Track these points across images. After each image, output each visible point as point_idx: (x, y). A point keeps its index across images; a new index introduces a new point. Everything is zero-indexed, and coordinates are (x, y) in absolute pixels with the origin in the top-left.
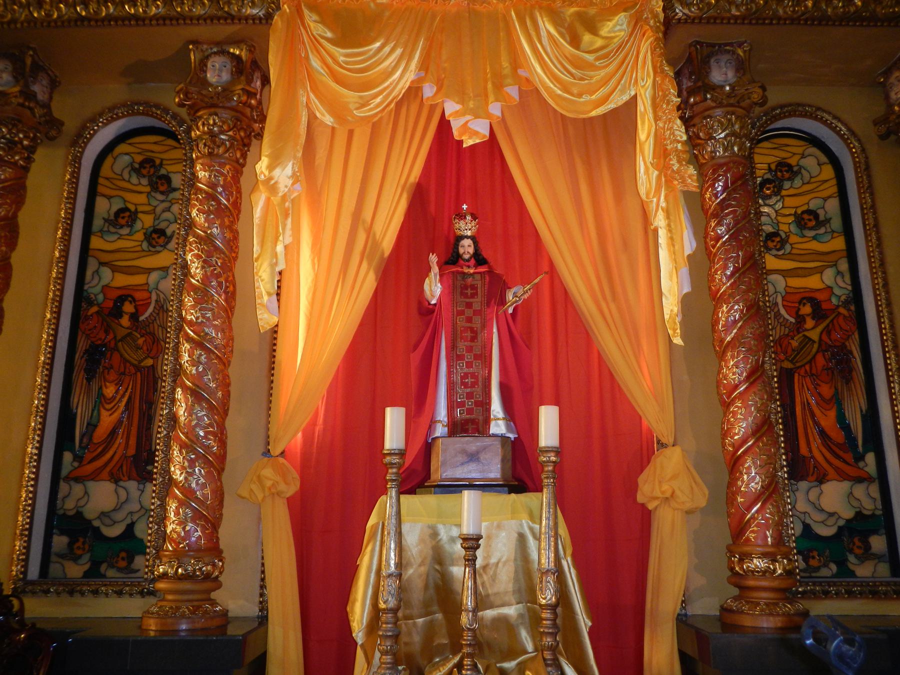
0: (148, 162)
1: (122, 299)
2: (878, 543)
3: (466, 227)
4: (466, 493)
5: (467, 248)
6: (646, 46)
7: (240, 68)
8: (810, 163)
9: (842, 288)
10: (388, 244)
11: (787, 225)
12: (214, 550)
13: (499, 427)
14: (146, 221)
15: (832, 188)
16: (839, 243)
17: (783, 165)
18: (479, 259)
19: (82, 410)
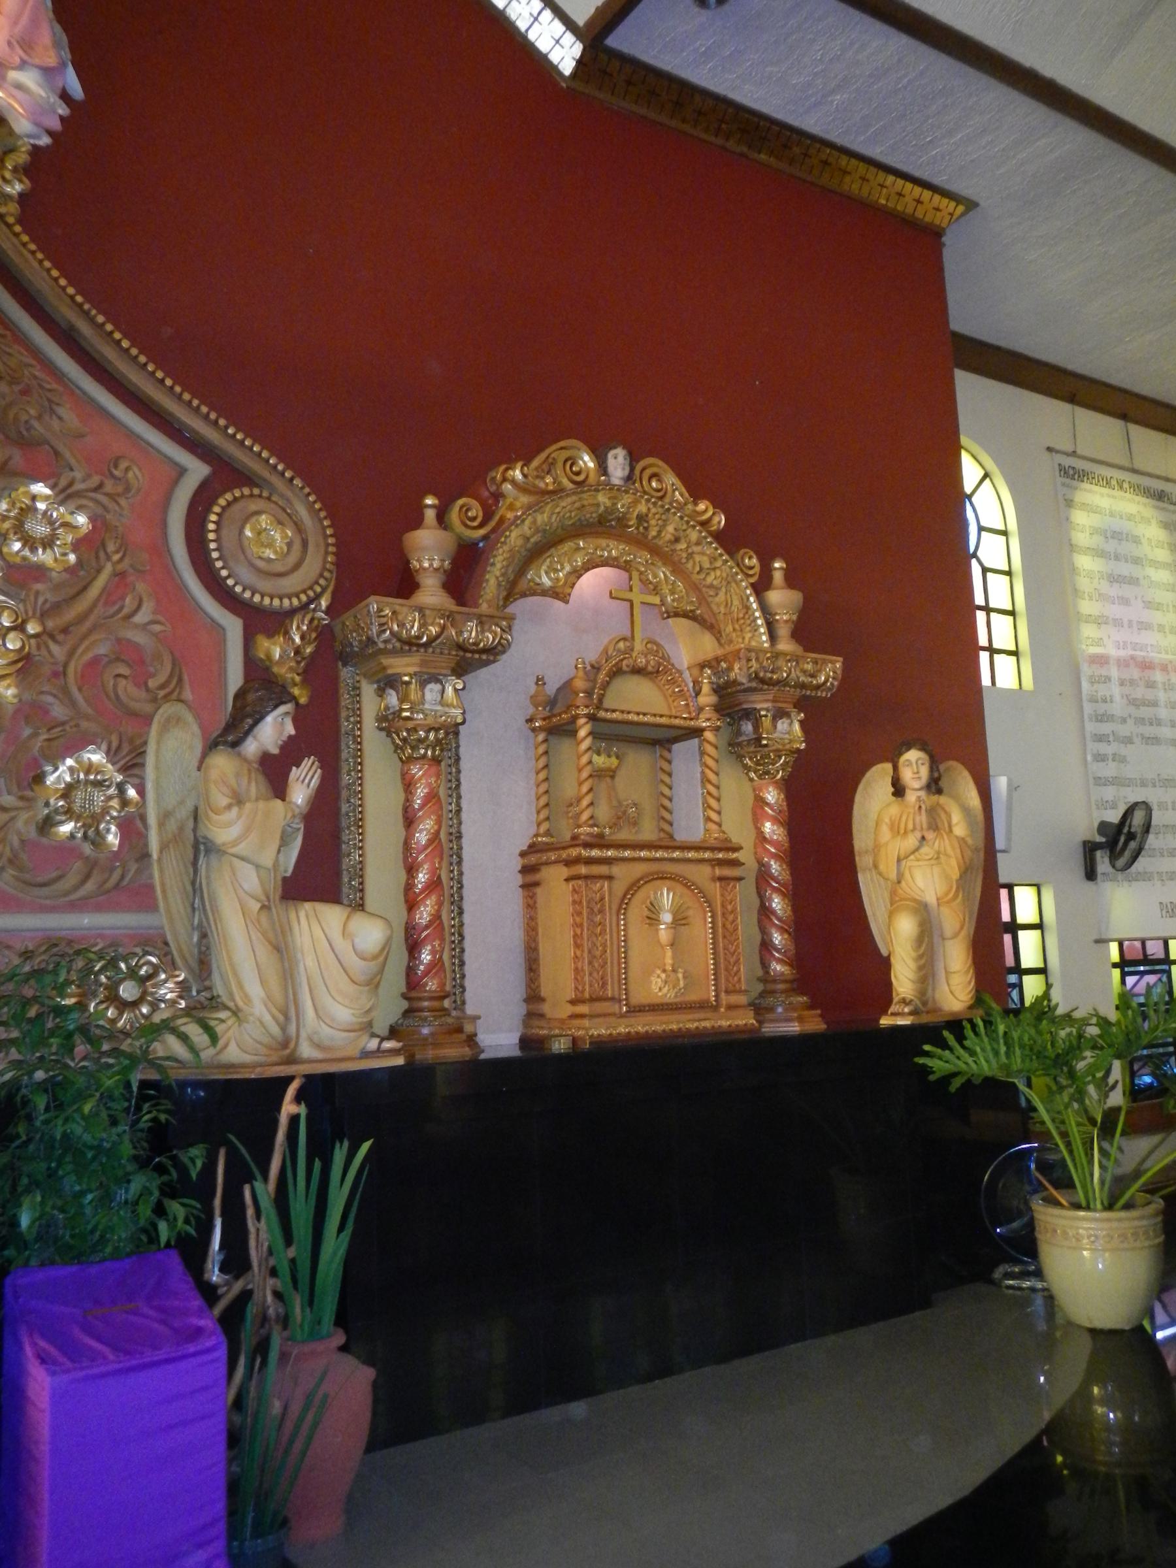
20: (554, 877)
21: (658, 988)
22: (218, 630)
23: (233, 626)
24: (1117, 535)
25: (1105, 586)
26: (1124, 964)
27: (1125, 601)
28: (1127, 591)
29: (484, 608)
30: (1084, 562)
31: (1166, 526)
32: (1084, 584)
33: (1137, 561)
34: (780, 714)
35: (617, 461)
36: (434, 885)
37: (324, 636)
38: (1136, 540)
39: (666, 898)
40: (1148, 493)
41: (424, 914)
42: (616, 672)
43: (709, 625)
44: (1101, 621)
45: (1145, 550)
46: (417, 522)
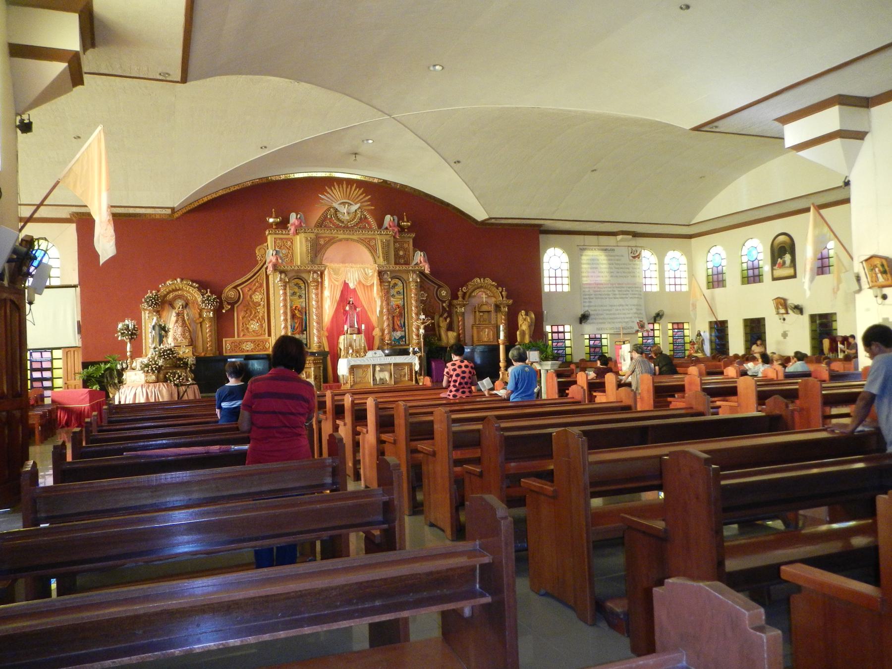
1: (296, 307)
2: (404, 339)
4: (354, 335)
5: (351, 302)
9: (402, 303)
11: (395, 294)
13: (356, 326)
14: (298, 294)
15: (402, 287)
16: (402, 297)
17: (395, 283)
20: (474, 327)
21: (485, 339)
22: (439, 304)
23: (440, 302)
24: (593, 260)
25: (589, 270)
26: (590, 339)
27: (594, 272)
28: (594, 270)
29: (466, 299)
30: (584, 266)
31: (606, 256)
32: (583, 270)
33: (598, 264)
34: (504, 307)
35: (482, 280)
38: (598, 260)
39: (487, 330)
40: (602, 250)
43: (495, 297)
44: (587, 277)
45: (601, 261)
46: (459, 291)
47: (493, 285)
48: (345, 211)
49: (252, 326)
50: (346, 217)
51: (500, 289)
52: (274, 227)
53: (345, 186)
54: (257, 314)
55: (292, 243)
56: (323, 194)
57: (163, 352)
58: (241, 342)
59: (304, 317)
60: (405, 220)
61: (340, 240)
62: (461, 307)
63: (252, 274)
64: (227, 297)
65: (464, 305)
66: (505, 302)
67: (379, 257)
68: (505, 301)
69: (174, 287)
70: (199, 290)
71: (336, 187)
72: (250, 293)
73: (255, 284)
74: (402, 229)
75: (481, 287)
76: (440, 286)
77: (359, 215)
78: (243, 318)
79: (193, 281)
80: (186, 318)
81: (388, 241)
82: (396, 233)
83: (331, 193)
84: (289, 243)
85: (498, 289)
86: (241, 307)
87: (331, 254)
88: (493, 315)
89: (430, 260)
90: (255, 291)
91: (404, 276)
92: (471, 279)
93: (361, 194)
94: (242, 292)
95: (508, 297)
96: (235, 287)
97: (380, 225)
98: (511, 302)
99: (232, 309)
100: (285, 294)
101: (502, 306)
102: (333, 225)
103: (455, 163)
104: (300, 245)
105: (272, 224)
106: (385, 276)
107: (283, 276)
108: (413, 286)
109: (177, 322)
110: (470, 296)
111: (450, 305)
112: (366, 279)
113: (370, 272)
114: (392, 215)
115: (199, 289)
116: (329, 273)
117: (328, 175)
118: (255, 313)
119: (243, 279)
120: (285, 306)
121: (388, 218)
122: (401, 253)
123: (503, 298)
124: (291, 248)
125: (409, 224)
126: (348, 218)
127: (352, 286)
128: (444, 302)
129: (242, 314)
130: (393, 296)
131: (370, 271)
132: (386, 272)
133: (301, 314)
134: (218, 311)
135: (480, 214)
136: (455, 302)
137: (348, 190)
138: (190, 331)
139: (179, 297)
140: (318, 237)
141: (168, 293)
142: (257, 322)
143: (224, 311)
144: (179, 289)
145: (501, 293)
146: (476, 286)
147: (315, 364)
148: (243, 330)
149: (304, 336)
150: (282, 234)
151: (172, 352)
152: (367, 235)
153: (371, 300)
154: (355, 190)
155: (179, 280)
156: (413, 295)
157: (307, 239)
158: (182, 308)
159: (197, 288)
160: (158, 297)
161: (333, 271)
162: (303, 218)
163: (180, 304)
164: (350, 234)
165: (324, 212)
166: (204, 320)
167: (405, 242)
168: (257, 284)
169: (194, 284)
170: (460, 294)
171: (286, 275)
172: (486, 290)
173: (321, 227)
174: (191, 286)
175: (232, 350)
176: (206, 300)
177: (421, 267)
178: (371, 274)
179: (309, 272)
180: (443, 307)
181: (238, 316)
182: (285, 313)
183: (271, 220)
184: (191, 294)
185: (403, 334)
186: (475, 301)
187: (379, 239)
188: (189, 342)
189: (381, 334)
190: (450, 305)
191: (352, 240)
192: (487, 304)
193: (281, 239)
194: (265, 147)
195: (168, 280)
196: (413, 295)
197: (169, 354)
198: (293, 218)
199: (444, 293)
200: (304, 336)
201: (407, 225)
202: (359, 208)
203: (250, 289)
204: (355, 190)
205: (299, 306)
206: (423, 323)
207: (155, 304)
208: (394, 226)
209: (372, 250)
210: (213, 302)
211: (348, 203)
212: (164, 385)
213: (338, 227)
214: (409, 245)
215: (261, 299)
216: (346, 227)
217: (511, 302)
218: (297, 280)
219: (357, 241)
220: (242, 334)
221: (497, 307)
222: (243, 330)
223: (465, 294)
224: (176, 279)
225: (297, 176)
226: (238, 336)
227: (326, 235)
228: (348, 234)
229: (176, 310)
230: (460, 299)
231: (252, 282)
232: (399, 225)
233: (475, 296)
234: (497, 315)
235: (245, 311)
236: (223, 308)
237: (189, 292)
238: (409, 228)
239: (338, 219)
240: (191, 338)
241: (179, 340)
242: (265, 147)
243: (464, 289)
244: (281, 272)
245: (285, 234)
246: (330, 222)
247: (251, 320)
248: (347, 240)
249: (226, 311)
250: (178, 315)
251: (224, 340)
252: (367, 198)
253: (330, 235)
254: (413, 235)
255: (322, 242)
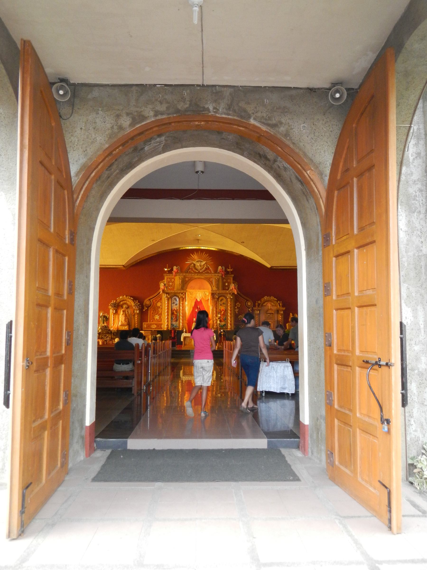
0: (175, 298)
3: (198, 306)
5: (198, 308)
6: (210, 295)
7: (183, 295)
8: (224, 299)
9: (225, 309)
10: (193, 306)
12: (183, 326)
18: (199, 308)
19: (172, 317)
29: (260, 307)
34: (281, 311)
35: (269, 297)
36: (258, 322)
37: (252, 309)
41: (257, 323)
42: (268, 310)
43: (275, 306)
46: (256, 303)
47: (275, 300)
48: (199, 265)
49: (156, 317)
50: (199, 268)
51: (279, 302)
52: (167, 272)
53: (199, 253)
54: (158, 312)
55: (174, 280)
56: (189, 257)
57: (102, 327)
58: (151, 324)
59: (178, 314)
60: (230, 268)
61: (196, 278)
62: (257, 311)
63: (157, 294)
64: (146, 304)
65: (259, 310)
66: (281, 309)
67: (214, 286)
68: (281, 308)
69: (123, 299)
70: (133, 301)
71: (196, 254)
72: (156, 303)
73: (158, 299)
74: (227, 273)
75: (268, 301)
76: (247, 300)
77: (205, 267)
78: (152, 313)
79: (131, 297)
80: (127, 313)
81: (219, 279)
82: (222, 275)
83: (193, 256)
84: (173, 280)
85: (277, 302)
86: (151, 309)
87: (191, 284)
88: (276, 315)
89: (239, 289)
90: (158, 301)
91: (226, 295)
92: (263, 297)
93: (208, 256)
94: (153, 301)
95: (283, 306)
96: (150, 300)
97: (216, 271)
98: (284, 309)
99: (147, 310)
100: (168, 303)
101: (280, 311)
102: (193, 271)
103: (242, 243)
104: (178, 281)
105: (166, 271)
106: (215, 296)
107: (167, 295)
108: (229, 300)
109: (123, 314)
110: (262, 306)
111: (253, 310)
112: (205, 297)
113: (207, 294)
114: (222, 267)
115: (133, 300)
116: (188, 294)
117: (198, 248)
118: (158, 311)
119: (153, 296)
120: (168, 309)
121: (220, 267)
122: (227, 284)
123: (280, 306)
124: (173, 282)
125: (232, 270)
126: (200, 268)
127: (199, 300)
128: (250, 308)
129: (152, 312)
130: (221, 305)
131: (207, 293)
132: (216, 294)
133: (177, 312)
134: (141, 310)
135: (269, 266)
136: (254, 308)
137: (201, 255)
138: (128, 319)
139: (125, 304)
140: (185, 277)
141: (121, 302)
142: (158, 316)
143: (144, 310)
144: (125, 300)
145: (279, 304)
146: (265, 301)
147: (151, 334)
148: (152, 319)
149: (178, 323)
150: (170, 276)
151: (106, 327)
152: (208, 276)
153: (208, 307)
154: (204, 255)
155: (125, 296)
156: (229, 305)
157: (180, 278)
158: (126, 308)
159: (132, 299)
160: (116, 304)
161: (190, 293)
162: (179, 268)
163: (125, 306)
164: (200, 276)
165: (189, 266)
166: (135, 314)
167: (229, 279)
168: (159, 298)
169: (131, 298)
170: (257, 304)
171: (169, 295)
172: (271, 303)
173: (187, 272)
174: (130, 299)
175: (146, 328)
176: (135, 305)
177: (233, 291)
178: (208, 295)
179: (179, 293)
180: (249, 311)
181: (150, 312)
182: (168, 312)
183: (166, 269)
184: (130, 302)
185: (225, 323)
186: (266, 308)
187: (215, 277)
188: (127, 323)
189: (213, 323)
190: (253, 310)
191: (201, 278)
192: (271, 309)
193: (169, 278)
194: (154, 240)
195: (121, 296)
196: (229, 305)
197: (105, 328)
198: (175, 268)
199: (249, 304)
200: (178, 323)
201: (231, 271)
202: (205, 264)
203: (156, 301)
204: (204, 255)
205: (175, 309)
206: (219, 319)
207: (114, 307)
208: (223, 271)
209: (211, 283)
210: (138, 306)
211: (201, 261)
212: (100, 340)
213: (196, 272)
214: (230, 280)
215: (161, 305)
216: (199, 272)
217: (284, 309)
218: (175, 297)
219: (204, 279)
220: (151, 321)
221: (278, 311)
222: (152, 319)
223: (259, 304)
224: (124, 296)
225: (187, 248)
226: (150, 322)
227: (190, 276)
228: (199, 276)
229: (123, 309)
230: (257, 307)
231: (156, 298)
232: (226, 270)
233: (265, 306)
234: (278, 315)
235: (154, 311)
236: (144, 309)
237: (129, 302)
238: (231, 272)
239: (196, 269)
240: (129, 321)
241: (123, 322)
242: (154, 240)
243: (259, 302)
244: (167, 293)
245: (171, 276)
246: (192, 270)
247: (156, 314)
248: (199, 278)
249: (145, 310)
250: (123, 311)
251: (144, 323)
252: (210, 258)
253: (191, 276)
254: (233, 275)
255: (187, 279)
